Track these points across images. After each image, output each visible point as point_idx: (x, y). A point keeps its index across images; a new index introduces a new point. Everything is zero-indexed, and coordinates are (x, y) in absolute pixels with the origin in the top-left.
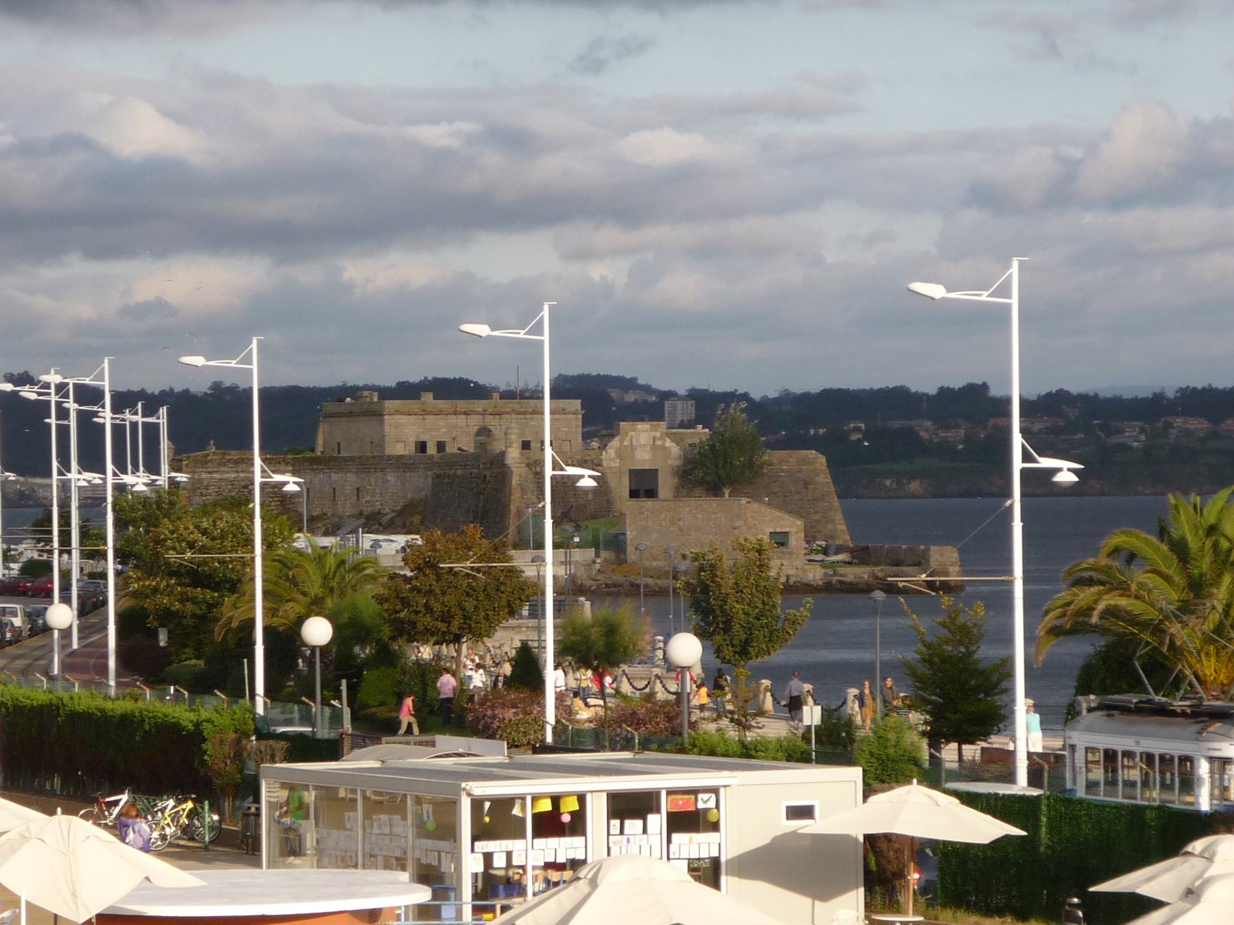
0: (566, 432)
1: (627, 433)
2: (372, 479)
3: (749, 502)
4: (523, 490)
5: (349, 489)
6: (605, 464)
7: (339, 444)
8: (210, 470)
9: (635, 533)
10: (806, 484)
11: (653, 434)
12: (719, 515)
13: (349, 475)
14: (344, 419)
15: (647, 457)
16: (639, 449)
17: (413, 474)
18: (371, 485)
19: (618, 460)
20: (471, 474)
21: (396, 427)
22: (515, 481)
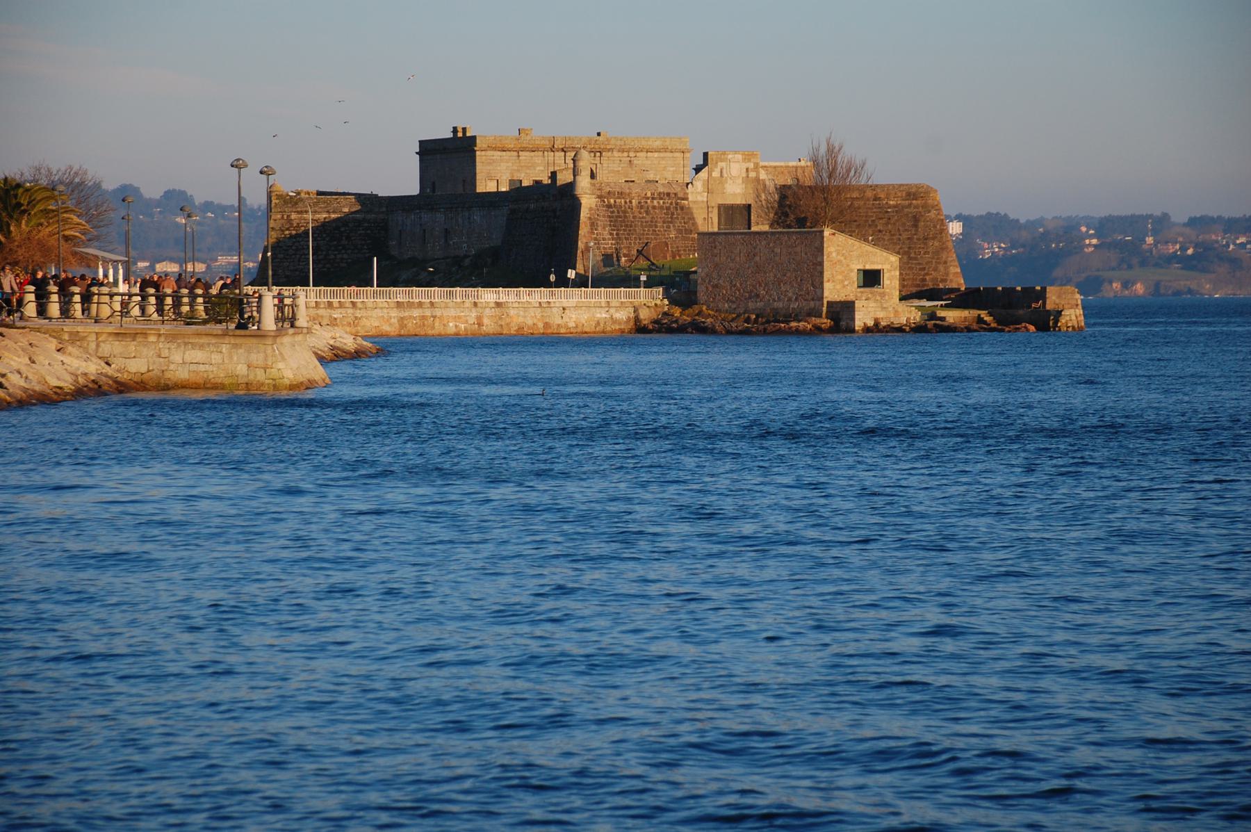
0: (673, 171)
1: (717, 163)
3: (834, 234)
4: (593, 225)
6: (691, 198)
7: (434, 183)
8: (299, 209)
9: (706, 270)
10: (916, 220)
12: (798, 249)
13: (438, 215)
14: (438, 156)
16: (729, 181)
20: (543, 208)
21: (490, 164)
22: (584, 214)
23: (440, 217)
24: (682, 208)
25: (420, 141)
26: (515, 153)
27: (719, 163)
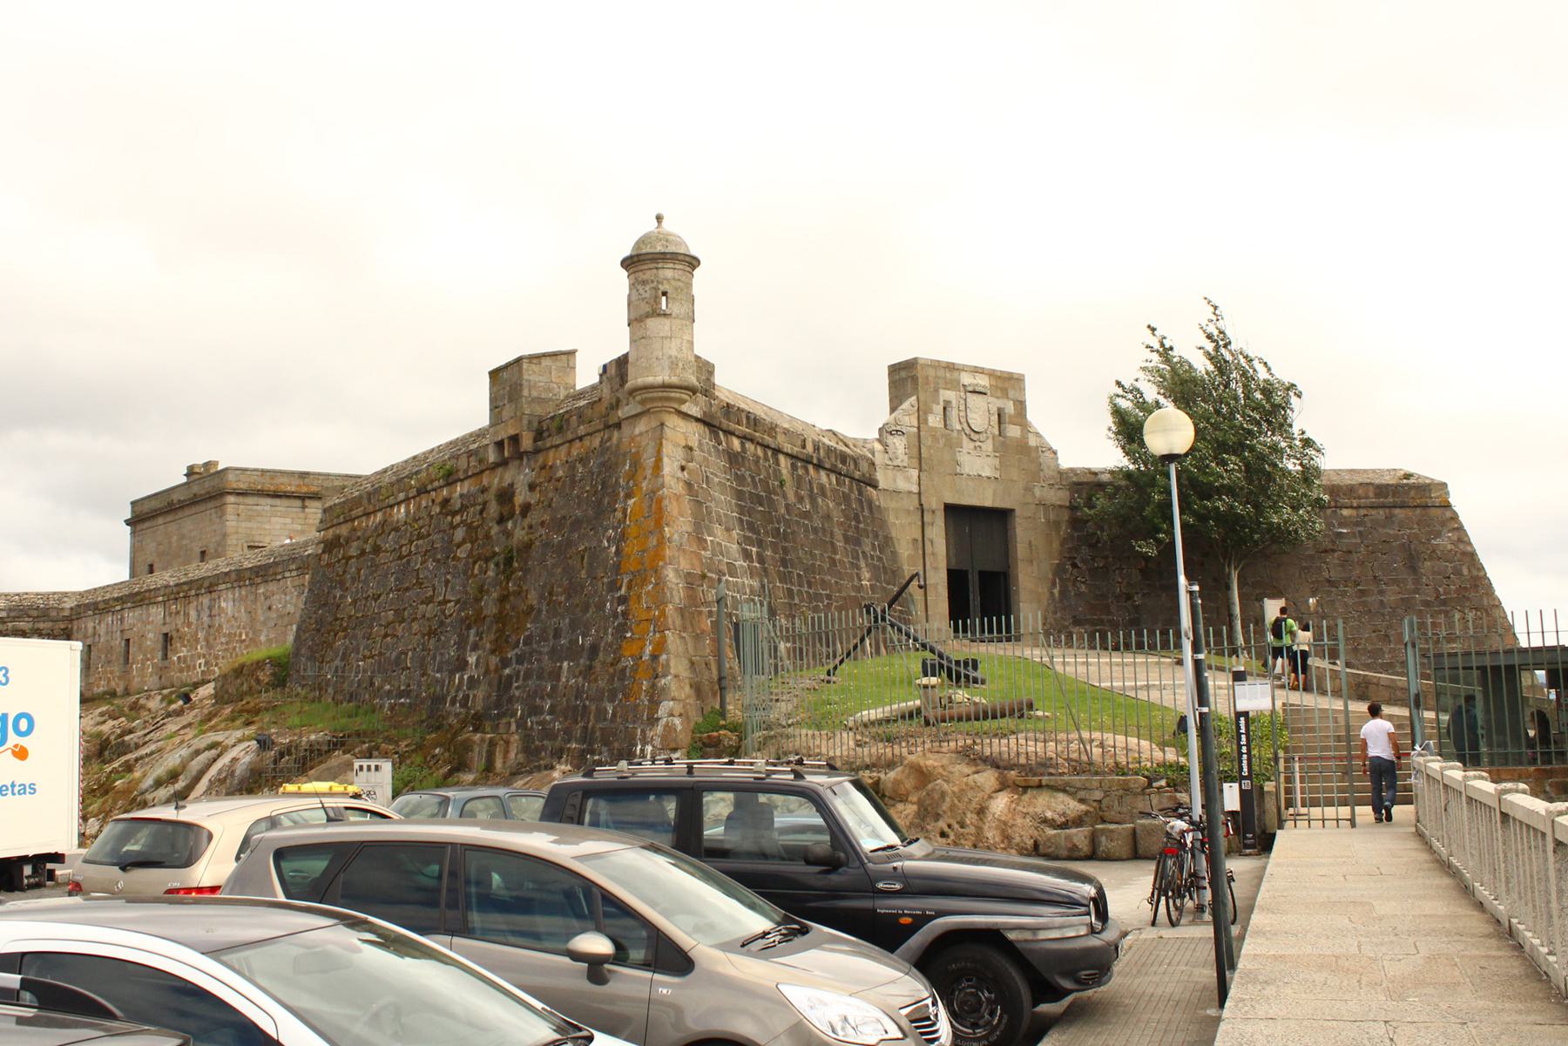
1: (936, 391)
2: (193, 613)
5: (152, 638)
11: (1000, 403)
13: (153, 610)
14: (160, 520)
15: (987, 472)
16: (967, 445)
17: (273, 587)
18: (189, 625)
19: (915, 473)
23: (156, 613)
24: (870, 503)
25: (134, 504)
26: (298, 503)
27: (941, 391)
